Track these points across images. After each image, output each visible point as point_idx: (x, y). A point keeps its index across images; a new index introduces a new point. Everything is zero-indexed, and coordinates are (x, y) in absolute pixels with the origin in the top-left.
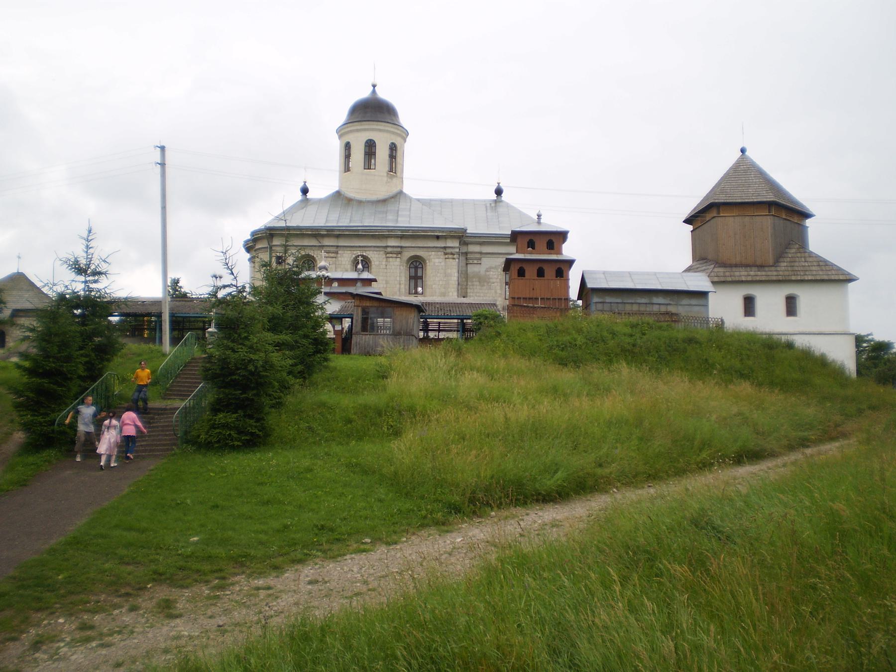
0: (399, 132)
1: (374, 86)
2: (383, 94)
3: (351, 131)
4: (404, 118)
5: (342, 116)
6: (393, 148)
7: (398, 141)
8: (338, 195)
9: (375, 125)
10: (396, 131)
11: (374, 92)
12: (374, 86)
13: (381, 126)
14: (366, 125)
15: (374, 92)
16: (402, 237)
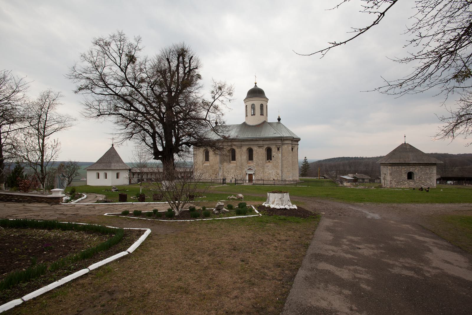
0: (264, 100)
1: (256, 84)
2: (259, 86)
3: (247, 101)
4: (267, 95)
5: (245, 95)
6: (262, 106)
7: (263, 103)
8: (244, 124)
9: (254, 98)
10: (264, 100)
11: (256, 85)
12: (256, 84)
13: (256, 98)
14: (251, 99)
15: (256, 85)
16: (263, 140)
